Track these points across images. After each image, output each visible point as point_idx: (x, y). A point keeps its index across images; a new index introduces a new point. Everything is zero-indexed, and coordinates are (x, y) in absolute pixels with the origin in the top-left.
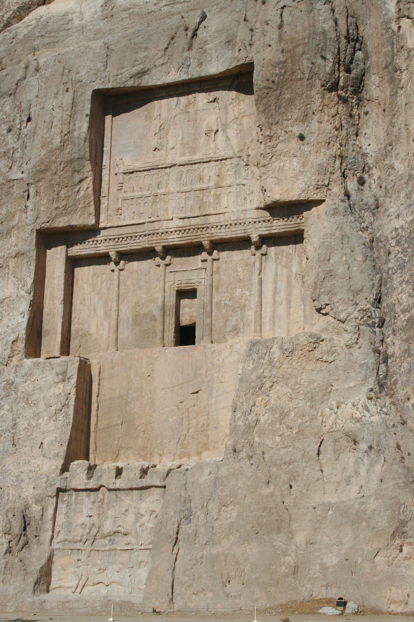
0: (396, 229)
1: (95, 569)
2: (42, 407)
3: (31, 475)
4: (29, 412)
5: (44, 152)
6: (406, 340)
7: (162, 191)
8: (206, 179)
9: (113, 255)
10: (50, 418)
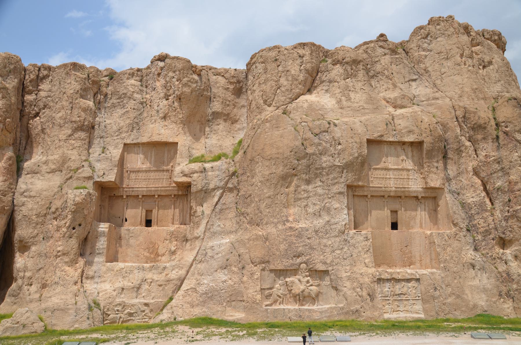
0: (473, 202)
1: (396, 306)
2: (360, 249)
3: (366, 273)
4: (356, 251)
5: (351, 158)
6: (484, 236)
7: (388, 177)
8: (403, 175)
9: (369, 196)
10: (365, 253)
